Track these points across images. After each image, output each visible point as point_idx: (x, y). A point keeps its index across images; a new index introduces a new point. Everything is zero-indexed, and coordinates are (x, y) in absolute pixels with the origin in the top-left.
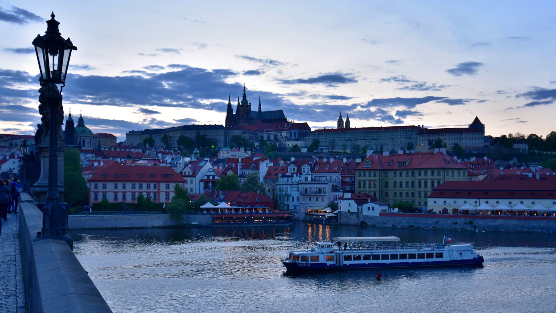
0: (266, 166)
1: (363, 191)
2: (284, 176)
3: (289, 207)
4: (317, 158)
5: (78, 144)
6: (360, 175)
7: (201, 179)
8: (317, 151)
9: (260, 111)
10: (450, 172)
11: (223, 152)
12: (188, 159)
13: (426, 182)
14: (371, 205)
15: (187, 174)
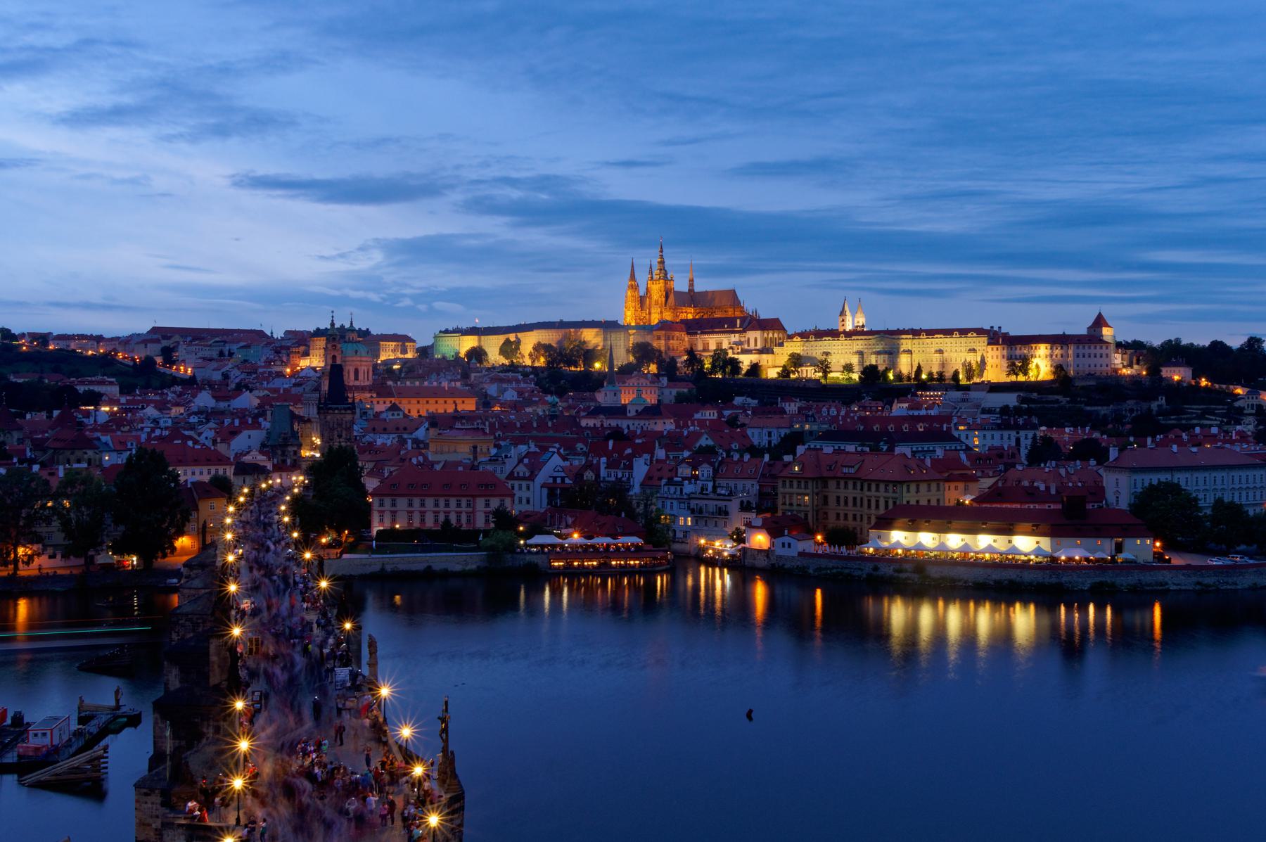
0: (646, 464)
1: (789, 511)
2: (670, 482)
3: (675, 533)
4: (724, 453)
5: (350, 404)
6: (784, 486)
7: (544, 483)
8: (797, 374)
9: (691, 290)
10: (913, 487)
11: (606, 394)
12: (523, 448)
13: (877, 502)
14: (786, 540)
15: (521, 475)
